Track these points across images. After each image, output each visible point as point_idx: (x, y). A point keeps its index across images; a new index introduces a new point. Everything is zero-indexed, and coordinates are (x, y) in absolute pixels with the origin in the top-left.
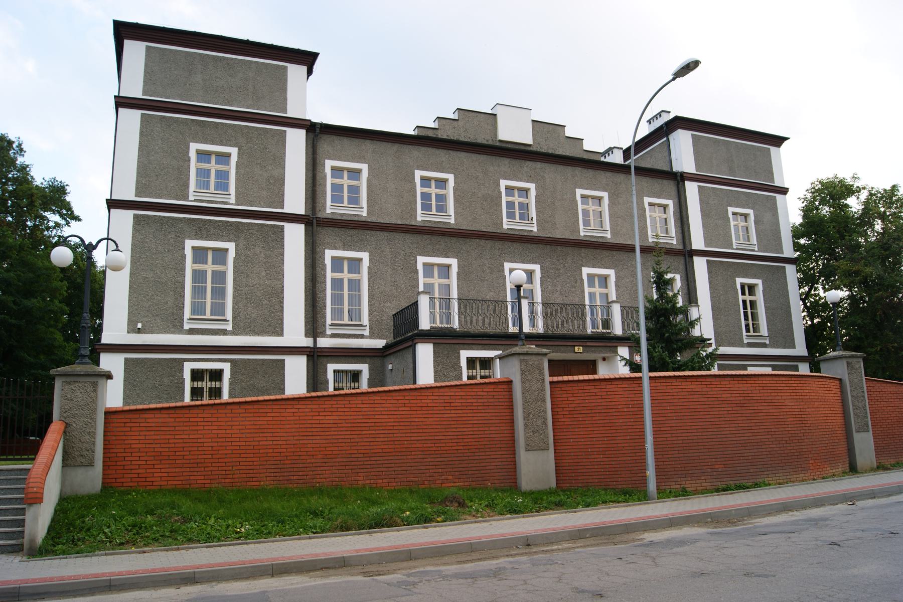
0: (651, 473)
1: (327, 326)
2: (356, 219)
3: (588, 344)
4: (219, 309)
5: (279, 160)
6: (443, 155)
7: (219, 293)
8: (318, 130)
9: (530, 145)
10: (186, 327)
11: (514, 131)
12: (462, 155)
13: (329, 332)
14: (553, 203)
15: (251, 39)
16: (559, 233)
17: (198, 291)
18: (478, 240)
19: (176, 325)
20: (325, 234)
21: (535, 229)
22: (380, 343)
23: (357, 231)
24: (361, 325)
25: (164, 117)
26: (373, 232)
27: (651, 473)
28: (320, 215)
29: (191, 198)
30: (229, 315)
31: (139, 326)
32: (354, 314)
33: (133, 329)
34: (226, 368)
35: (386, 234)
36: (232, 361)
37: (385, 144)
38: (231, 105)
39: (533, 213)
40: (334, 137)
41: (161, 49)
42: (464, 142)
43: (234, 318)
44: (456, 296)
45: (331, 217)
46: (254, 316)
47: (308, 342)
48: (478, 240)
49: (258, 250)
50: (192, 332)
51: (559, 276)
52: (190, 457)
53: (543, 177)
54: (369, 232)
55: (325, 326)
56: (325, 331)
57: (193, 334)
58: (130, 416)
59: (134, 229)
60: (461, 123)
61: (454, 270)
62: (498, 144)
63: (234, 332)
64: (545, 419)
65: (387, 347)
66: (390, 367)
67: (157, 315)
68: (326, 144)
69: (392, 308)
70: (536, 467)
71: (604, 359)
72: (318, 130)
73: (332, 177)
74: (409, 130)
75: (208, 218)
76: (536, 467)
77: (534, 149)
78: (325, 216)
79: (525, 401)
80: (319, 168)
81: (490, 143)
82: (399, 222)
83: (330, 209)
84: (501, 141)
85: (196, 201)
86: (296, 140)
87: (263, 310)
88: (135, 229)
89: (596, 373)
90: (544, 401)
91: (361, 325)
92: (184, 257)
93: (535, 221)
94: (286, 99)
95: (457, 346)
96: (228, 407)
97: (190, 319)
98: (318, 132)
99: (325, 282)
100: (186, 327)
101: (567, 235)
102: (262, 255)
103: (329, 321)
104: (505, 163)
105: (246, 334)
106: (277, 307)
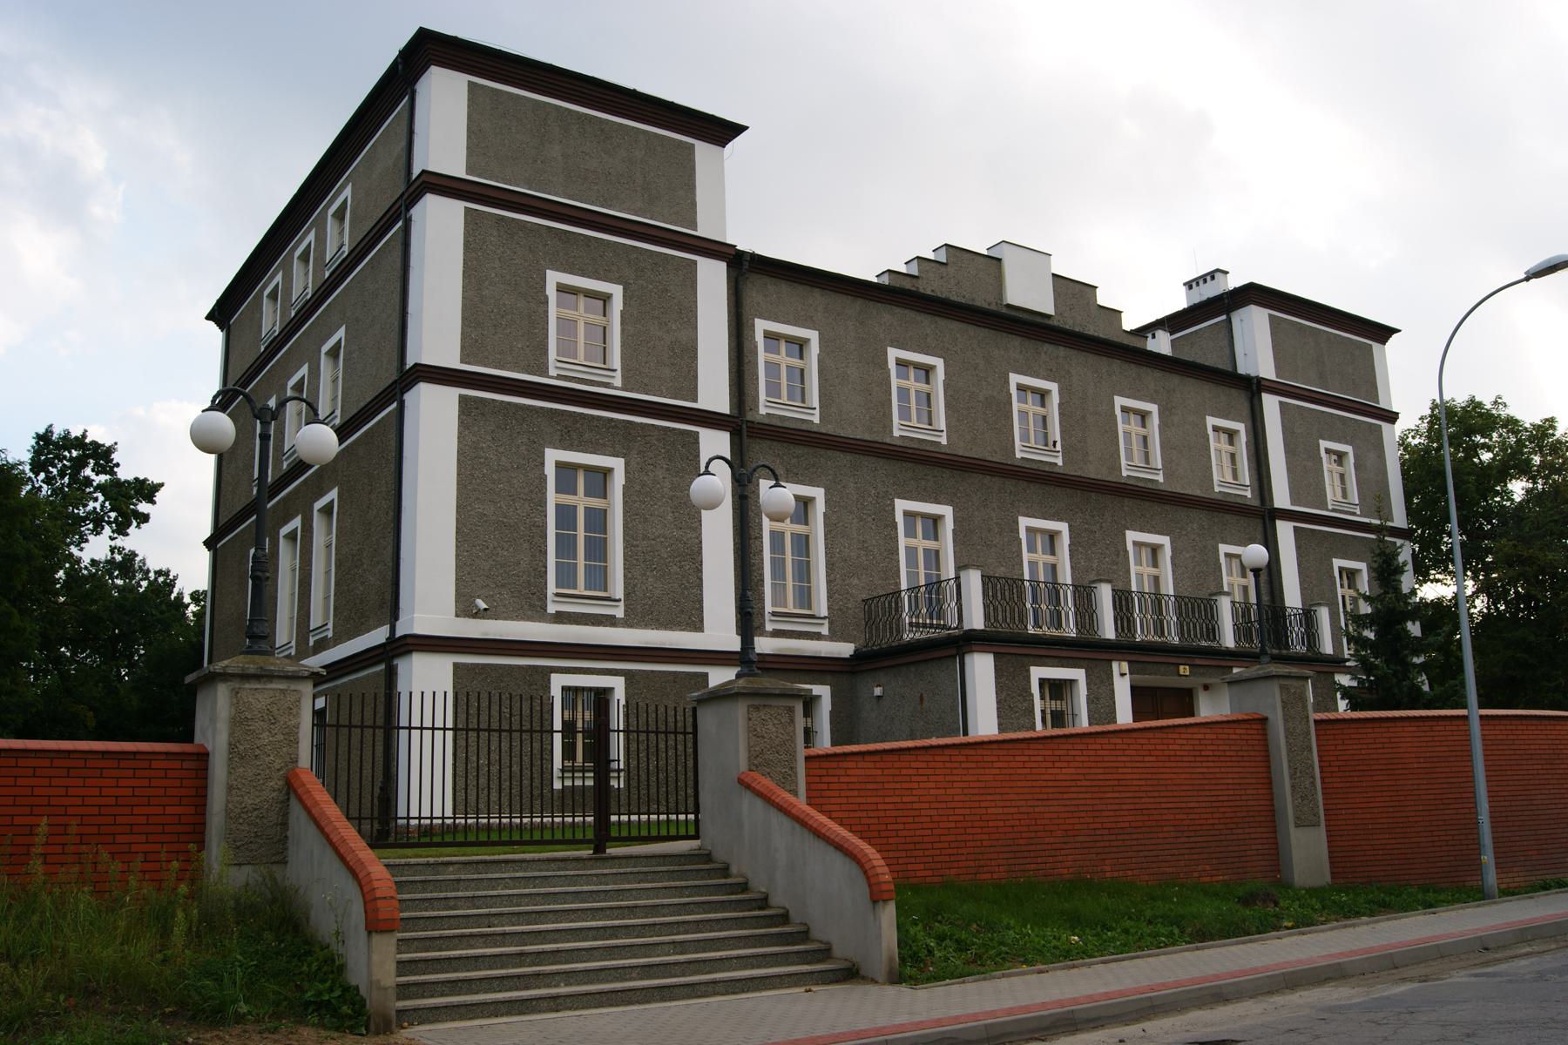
0: (1488, 858)
1: (767, 617)
2: (804, 427)
3: (1198, 662)
4: (599, 577)
5: (687, 314)
6: (926, 324)
7: (597, 549)
8: (746, 265)
9: (1049, 317)
10: (552, 609)
11: (1027, 292)
12: (955, 326)
13: (769, 627)
14: (1084, 417)
15: (640, 89)
16: (1092, 471)
17: (566, 545)
18: (977, 474)
19: (534, 608)
20: (761, 453)
21: (1060, 462)
22: (845, 649)
23: (806, 450)
24: (812, 617)
25: (503, 217)
26: (830, 453)
27: (1488, 858)
28: (749, 416)
29: (553, 372)
30: (618, 590)
31: (482, 605)
32: (805, 596)
33: (465, 609)
34: (618, 685)
35: (849, 457)
36: (627, 675)
37: (844, 298)
38: (609, 207)
39: (1056, 433)
40: (766, 279)
41: (493, 90)
42: (953, 301)
43: (627, 595)
44: (1069, 581)
45: (766, 421)
46: (657, 592)
47: (733, 643)
48: (977, 474)
49: (660, 474)
50: (560, 618)
51: (1094, 544)
52: (905, 833)
53: (1068, 372)
54: (823, 452)
55: (763, 615)
56: (763, 624)
57: (561, 622)
58: (825, 764)
59: (461, 423)
60: (951, 270)
61: (949, 525)
62: (1004, 310)
63: (628, 622)
64: (1313, 777)
65: (857, 656)
66: (878, 691)
67: (503, 586)
68: (754, 292)
69: (860, 589)
70: (1307, 852)
71: (1206, 687)
72: (746, 265)
73: (766, 350)
74: (867, 271)
75: (580, 412)
76: (1307, 852)
77: (1054, 323)
78: (758, 419)
79: (1289, 751)
80: (746, 332)
81: (993, 307)
82: (867, 437)
83: (764, 407)
84: (1009, 306)
85: (559, 377)
86: (712, 277)
87: (668, 587)
88: (463, 424)
89: (1192, 715)
90: (1310, 750)
91: (812, 617)
92: (544, 479)
93: (1059, 447)
94: (694, 204)
95: (1026, 660)
96: (947, 752)
97: (557, 595)
98: (747, 268)
99: (761, 537)
100: (552, 609)
101: (1102, 474)
102: (667, 484)
103: (769, 608)
104: (1014, 346)
105: (646, 626)
106: (692, 579)
